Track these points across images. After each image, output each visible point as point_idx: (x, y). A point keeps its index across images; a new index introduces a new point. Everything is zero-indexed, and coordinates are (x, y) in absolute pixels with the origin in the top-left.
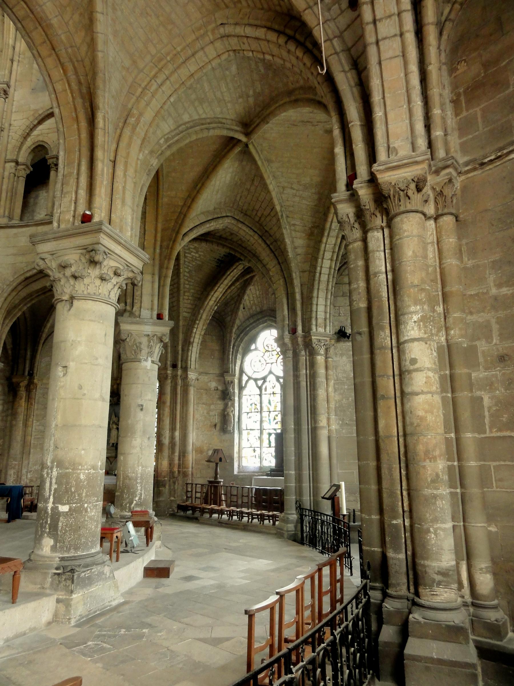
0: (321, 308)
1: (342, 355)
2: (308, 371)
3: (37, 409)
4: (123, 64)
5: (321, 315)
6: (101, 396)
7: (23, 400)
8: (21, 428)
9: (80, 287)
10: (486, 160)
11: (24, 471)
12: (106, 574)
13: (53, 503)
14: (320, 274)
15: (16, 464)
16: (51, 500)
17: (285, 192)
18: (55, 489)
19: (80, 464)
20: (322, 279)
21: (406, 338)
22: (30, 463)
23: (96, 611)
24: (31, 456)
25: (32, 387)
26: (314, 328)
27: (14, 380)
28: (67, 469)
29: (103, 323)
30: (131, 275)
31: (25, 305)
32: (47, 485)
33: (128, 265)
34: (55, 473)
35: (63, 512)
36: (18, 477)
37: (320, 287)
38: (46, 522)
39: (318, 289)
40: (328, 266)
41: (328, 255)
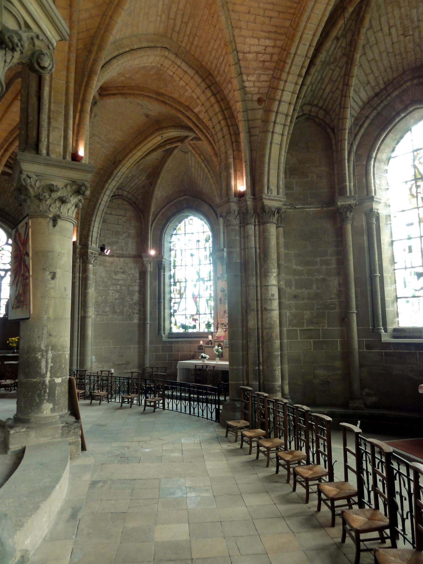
0: (95, 229)
1: (100, 265)
2: (81, 275)
5: (95, 235)
9: (64, 209)
10: (297, 207)
14: (100, 204)
16: (48, 374)
17: (93, 138)
18: (51, 367)
20: (100, 209)
21: (270, 284)
26: (90, 243)
28: (59, 351)
32: (43, 364)
34: (50, 354)
35: (58, 383)
37: (98, 214)
38: (45, 392)
39: (96, 215)
40: (106, 200)
41: (108, 192)
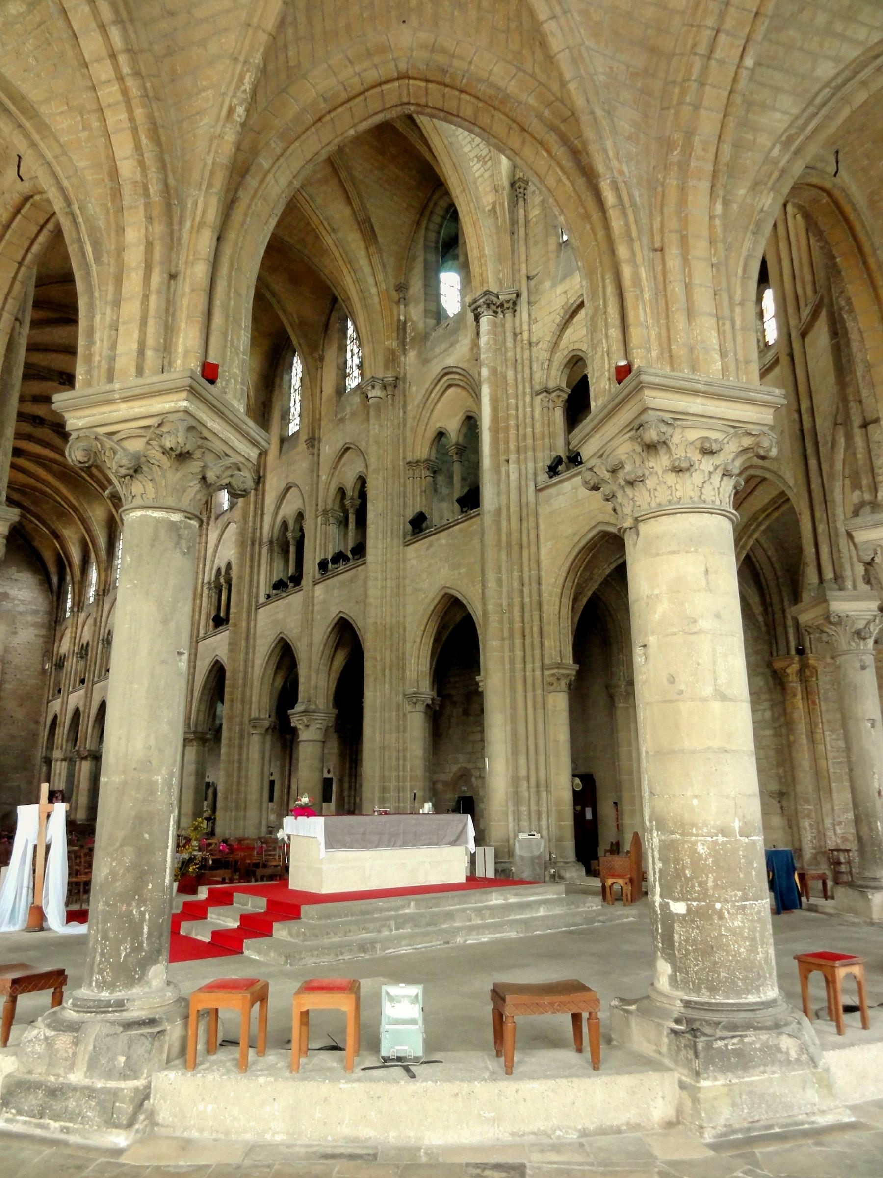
3: (827, 711)
4: (631, 69)
6: (716, 690)
7: (799, 696)
8: (806, 747)
9: (642, 498)
11: (828, 822)
12: (787, 1053)
13: (661, 896)
15: (810, 810)
18: (661, 871)
19: (693, 825)
22: (836, 808)
23: (771, 1127)
24: (835, 795)
25: (808, 673)
27: (778, 665)
28: (672, 833)
29: (696, 551)
30: (747, 442)
31: (750, 537)
33: (736, 427)
35: (677, 915)
36: (819, 832)
